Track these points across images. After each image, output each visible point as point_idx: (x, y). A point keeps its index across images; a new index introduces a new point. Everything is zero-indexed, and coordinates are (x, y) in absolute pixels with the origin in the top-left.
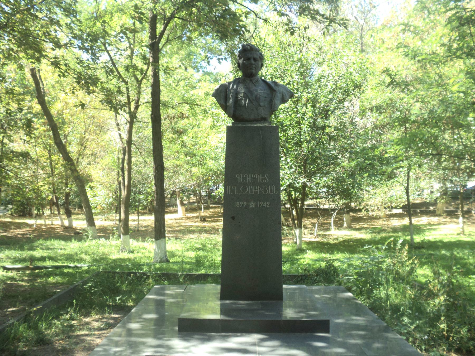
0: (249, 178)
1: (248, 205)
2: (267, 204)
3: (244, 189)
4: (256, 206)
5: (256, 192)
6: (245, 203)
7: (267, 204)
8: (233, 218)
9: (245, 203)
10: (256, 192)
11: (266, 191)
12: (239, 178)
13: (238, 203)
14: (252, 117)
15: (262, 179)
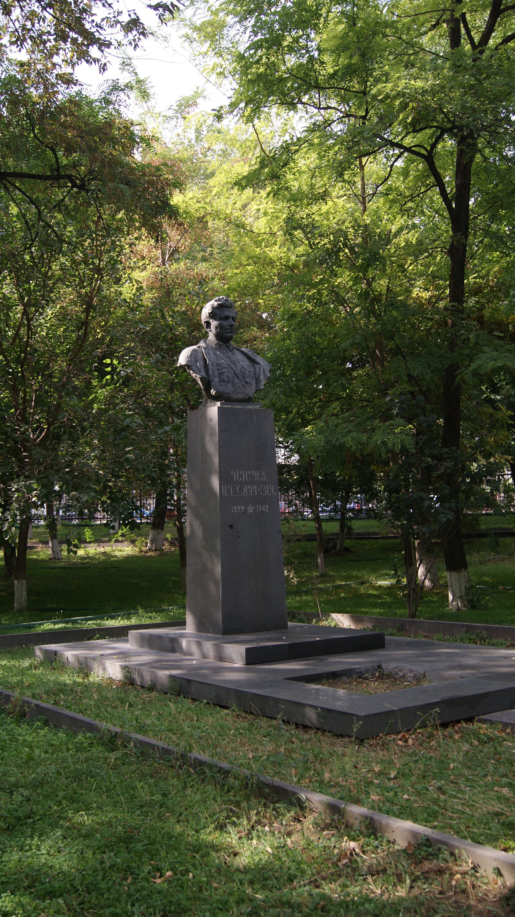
0: (245, 476)
1: (246, 510)
2: (266, 508)
3: (241, 489)
4: (255, 510)
5: (254, 493)
6: (243, 508)
7: (266, 508)
8: (231, 527)
9: (243, 508)
10: (254, 493)
11: (263, 492)
12: (236, 476)
13: (235, 508)
14: (240, 396)
15: (260, 477)
